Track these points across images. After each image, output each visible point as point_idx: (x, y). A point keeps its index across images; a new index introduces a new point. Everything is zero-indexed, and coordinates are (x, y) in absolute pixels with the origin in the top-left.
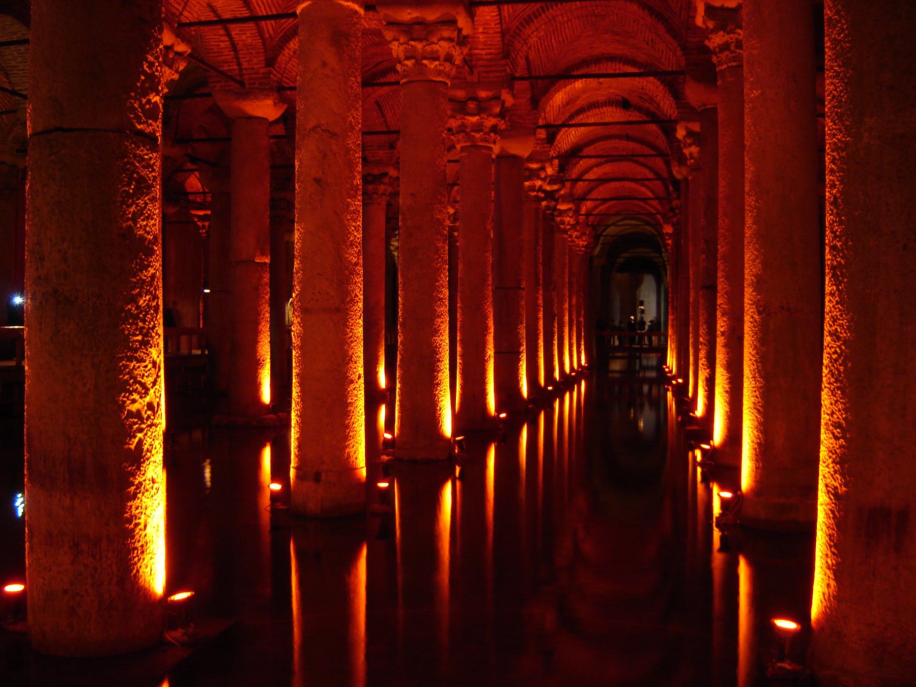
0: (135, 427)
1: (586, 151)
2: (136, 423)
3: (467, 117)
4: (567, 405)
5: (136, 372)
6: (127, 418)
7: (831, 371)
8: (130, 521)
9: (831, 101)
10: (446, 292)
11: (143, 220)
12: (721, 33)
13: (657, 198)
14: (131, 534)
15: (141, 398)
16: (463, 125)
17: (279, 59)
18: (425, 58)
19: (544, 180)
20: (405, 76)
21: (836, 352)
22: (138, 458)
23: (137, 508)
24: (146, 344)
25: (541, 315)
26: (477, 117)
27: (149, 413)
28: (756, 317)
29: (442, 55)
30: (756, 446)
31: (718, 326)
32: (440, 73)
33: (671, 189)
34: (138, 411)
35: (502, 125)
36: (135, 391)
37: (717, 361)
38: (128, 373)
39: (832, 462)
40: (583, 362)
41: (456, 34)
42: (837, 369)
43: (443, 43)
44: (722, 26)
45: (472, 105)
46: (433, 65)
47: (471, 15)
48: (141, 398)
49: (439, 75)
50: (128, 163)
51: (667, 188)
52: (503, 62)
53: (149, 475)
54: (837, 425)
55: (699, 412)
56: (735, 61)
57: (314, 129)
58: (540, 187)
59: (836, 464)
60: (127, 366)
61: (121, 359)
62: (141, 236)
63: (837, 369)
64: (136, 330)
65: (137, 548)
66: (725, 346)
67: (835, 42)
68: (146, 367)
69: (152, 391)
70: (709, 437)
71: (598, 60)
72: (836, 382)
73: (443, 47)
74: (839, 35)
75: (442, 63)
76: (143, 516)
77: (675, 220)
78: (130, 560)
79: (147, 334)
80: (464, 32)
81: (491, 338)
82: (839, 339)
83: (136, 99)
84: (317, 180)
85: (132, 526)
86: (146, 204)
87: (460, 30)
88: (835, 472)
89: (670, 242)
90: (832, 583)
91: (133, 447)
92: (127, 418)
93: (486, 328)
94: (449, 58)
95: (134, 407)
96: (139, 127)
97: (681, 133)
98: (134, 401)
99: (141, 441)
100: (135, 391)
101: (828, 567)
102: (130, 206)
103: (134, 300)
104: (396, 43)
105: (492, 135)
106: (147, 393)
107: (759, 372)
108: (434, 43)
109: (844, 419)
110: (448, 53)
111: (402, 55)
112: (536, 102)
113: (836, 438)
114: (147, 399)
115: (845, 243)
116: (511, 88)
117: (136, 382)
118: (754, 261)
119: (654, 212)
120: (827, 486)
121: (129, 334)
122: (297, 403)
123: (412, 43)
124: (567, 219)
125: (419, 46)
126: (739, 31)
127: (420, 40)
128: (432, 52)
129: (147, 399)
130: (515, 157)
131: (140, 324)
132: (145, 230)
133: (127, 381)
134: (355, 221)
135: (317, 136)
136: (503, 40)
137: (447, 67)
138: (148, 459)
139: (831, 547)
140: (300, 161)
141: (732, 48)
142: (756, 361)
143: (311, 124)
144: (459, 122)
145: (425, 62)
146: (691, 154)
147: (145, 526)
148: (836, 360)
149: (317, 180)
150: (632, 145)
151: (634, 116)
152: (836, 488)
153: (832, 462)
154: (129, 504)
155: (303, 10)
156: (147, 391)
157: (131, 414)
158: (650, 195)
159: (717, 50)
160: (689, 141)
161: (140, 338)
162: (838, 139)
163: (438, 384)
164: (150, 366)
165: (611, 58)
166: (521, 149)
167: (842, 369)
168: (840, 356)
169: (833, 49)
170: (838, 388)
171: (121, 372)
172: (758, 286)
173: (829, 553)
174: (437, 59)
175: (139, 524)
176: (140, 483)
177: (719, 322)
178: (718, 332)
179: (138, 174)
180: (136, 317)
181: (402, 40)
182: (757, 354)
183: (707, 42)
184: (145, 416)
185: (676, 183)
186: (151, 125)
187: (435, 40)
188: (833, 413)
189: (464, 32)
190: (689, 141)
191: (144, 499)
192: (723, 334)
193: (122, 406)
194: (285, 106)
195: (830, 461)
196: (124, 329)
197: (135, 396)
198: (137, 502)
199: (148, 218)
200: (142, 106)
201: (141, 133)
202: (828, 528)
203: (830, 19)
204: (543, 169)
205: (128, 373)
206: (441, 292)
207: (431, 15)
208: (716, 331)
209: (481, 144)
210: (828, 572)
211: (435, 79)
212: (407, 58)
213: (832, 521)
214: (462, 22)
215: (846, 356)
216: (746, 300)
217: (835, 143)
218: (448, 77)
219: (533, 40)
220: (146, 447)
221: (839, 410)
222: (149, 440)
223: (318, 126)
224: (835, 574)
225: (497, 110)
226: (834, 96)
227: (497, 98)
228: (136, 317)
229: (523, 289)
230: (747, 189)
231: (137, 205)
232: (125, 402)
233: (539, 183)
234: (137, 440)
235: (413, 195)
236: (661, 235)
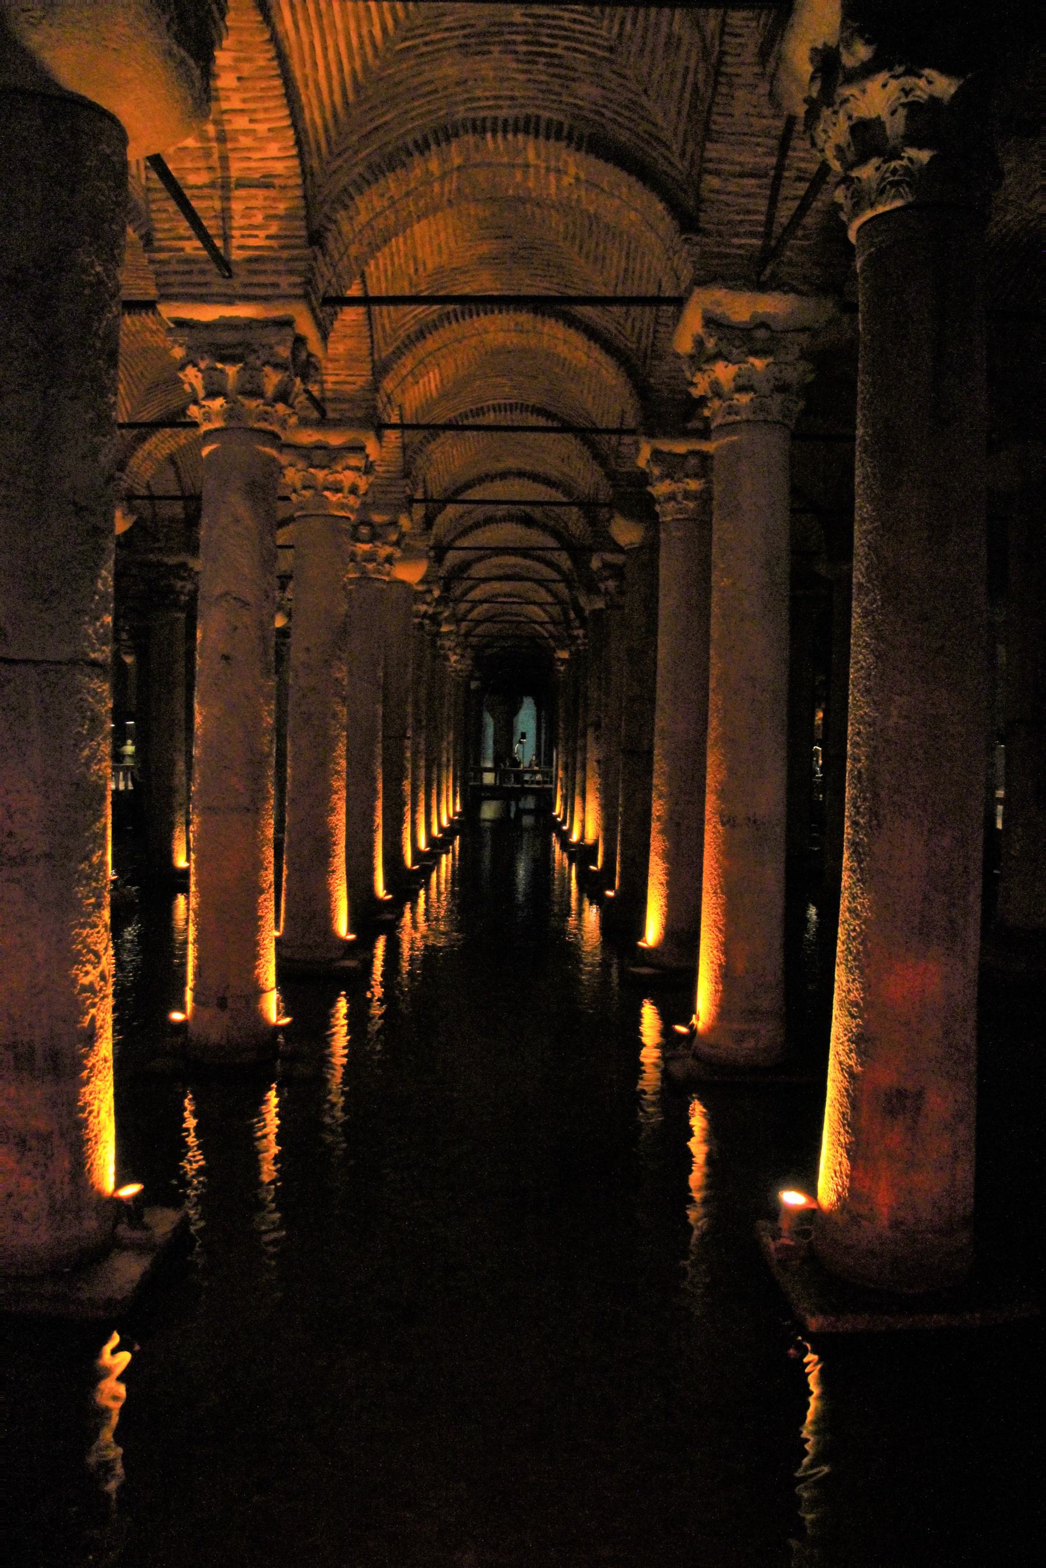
0: (88, 1002)
1: (478, 570)
2: (88, 998)
3: (359, 545)
4: (445, 860)
5: (89, 940)
6: (79, 994)
7: (848, 948)
8: (83, 1109)
9: (857, 671)
10: (343, 763)
11: (96, 764)
12: (668, 481)
13: (553, 622)
14: (83, 1124)
15: (94, 968)
17: (131, 463)
18: (327, 489)
19: (428, 604)
20: (302, 509)
21: (854, 930)
22: (90, 1037)
23: (91, 1094)
24: (99, 906)
25: (422, 763)
26: (371, 545)
27: (102, 983)
28: (720, 827)
29: (347, 485)
30: (716, 967)
31: (653, 810)
32: (343, 506)
33: (572, 615)
34: (92, 984)
35: (398, 554)
36: (89, 961)
37: (652, 848)
38: (82, 942)
39: (848, 1041)
40: (458, 808)
41: (364, 462)
42: (856, 947)
43: (348, 473)
44: (669, 476)
46: (333, 497)
47: (379, 438)
48: (94, 968)
49: (342, 509)
50: (81, 699)
51: (565, 613)
52: (403, 482)
53: (102, 1055)
54: (855, 1004)
55: (653, 932)
56: (681, 513)
58: (426, 612)
59: (853, 1042)
60: (79, 935)
61: (74, 927)
62: (94, 782)
63: (858, 950)
64: (89, 892)
65: (89, 1140)
66: (662, 832)
67: (866, 613)
68: (98, 932)
69: (104, 959)
70: (640, 933)
71: (503, 475)
72: (855, 959)
73: (348, 478)
74: (872, 604)
75: (346, 494)
76: (96, 1102)
77: (573, 648)
78: (84, 1153)
79: (99, 896)
80: (371, 459)
81: (379, 804)
82: (858, 916)
83: (90, 623)
84: (226, 658)
85: (86, 1115)
86: (99, 744)
87: (367, 456)
88: (851, 1051)
89: (562, 668)
90: (845, 1161)
91: (86, 1025)
92: (79, 994)
93: (375, 790)
94: (354, 490)
95: (86, 981)
96: (93, 656)
97: (595, 564)
98: (87, 973)
99: (93, 1019)
100: (89, 961)
101: (841, 1145)
102: (82, 750)
103: (87, 857)
104: (293, 470)
105: (387, 566)
106: (99, 963)
107: (721, 887)
108: (337, 472)
109: (862, 999)
110: (353, 484)
111: (299, 485)
112: (429, 522)
113: (853, 1017)
114: (100, 968)
115: (870, 821)
116: (410, 513)
117: (90, 951)
118: (719, 766)
119: (546, 635)
120: (840, 1063)
121: (82, 898)
122: (197, 915)
123: (312, 470)
124: (448, 644)
125: (321, 475)
126: (687, 480)
127: (323, 468)
128: (335, 482)
129: (100, 968)
130: (403, 582)
131: (94, 884)
132: (97, 775)
133: (79, 951)
134: (268, 704)
136: (404, 455)
137: (353, 501)
138: (101, 1037)
139: (844, 1125)
140: (204, 632)
141: (680, 498)
142: (718, 875)
143: (218, 591)
145: (326, 493)
146: (606, 589)
147: (99, 1113)
148: (854, 938)
149: (226, 658)
150: (528, 562)
151: (536, 538)
152: (851, 1066)
153: (848, 1041)
154: (83, 1090)
155: (210, 453)
156: (98, 956)
157: (85, 989)
158: (543, 614)
159: (662, 499)
160: (605, 574)
161: (93, 900)
162: (866, 713)
163: (333, 872)
164: (103, 930)
165: (521, 474)
166: (411, 573)
167: (861, 948)
168: (859, 934)
169: (863, 617)
170: (857, 967)
171: (74, 942)
172: (722, 794)
173: (842, 1130)
174: (338, 490)
175: (91, 1112)
176: (94, 1065)
177: (654, 805)
178: (654, 817)
179: (92, 710)
180: (89, 878)
181: (300, 466)
182: (720, 868)
183: (649, 489)
184: (98, 988)
185: (579, 610)
186: (104, 651)
187: (339, 468)
188: (849, 991)
189: (371, 459)
190: (605, 574)
191: (98, 1083)
192: (659, 818)
193: (74, 981)
194: (135, 517)
195: (845, 1039)
196: (77, 892)
197: (89, 967)
198: (91, 1087)
199: (100, 761)
200: (96, 632)
201: (94, 664)
202: (841, 1105)
203: (860, 585)
204: (430, 591)
205: (82, 942)
206: (338, 764)
207: (335, 439)
208: (650, 815)
209: (374, 576)
210: (840, 1150)
211: (336, 513)
212: (305, 488)
213: (845, 1100)
214: (372, 448)
215: (866, 935)
216: (708, 808)
217: (862, 717)
218: (352, 511)
219: (437, 455)
220: (98, 1024)
221: (857, 989)
222: (102, 1015)
223: (227, 593)
224: (848, 1153)
225: (394, 537)
226: (862, 667)
227: (394, 523)
228: (89, 878)
229: (409, 738)
230: (712, 685)
231: (91, 748)
232: (77, 975)
233: (423, 608)
234: (88, 1017)
235: (308, 650)
236: (552, 660)
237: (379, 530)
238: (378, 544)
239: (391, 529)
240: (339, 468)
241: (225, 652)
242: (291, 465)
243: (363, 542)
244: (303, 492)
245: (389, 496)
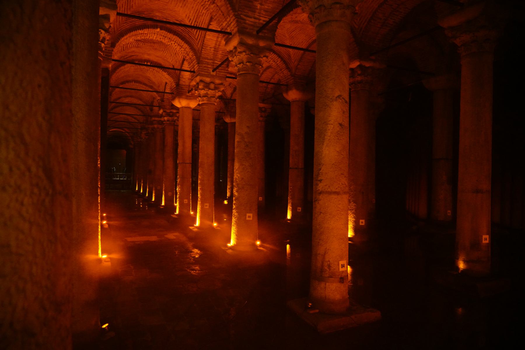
16: (207, 93)
18: (256, 64)
45: (212, 86)
57: (339, 96)
84: (341, 125)
104: (244, 53)
111: (245, 60)
123: (252, 55)
135: (340, 101)
143: (337, 95)
144: (205, 92)
145: (256, 65)
149: (341, 125)
181: (247, 53)
187: (262, 56)
212: (249, 62)
237: (216, 86)
238: (217, 91)
239: (221, 86)
240: (262, 56)
241: (341, 122)
242: (244, 52)
243: (212, 90)
244: (248, 64)
245: (222, 73)
